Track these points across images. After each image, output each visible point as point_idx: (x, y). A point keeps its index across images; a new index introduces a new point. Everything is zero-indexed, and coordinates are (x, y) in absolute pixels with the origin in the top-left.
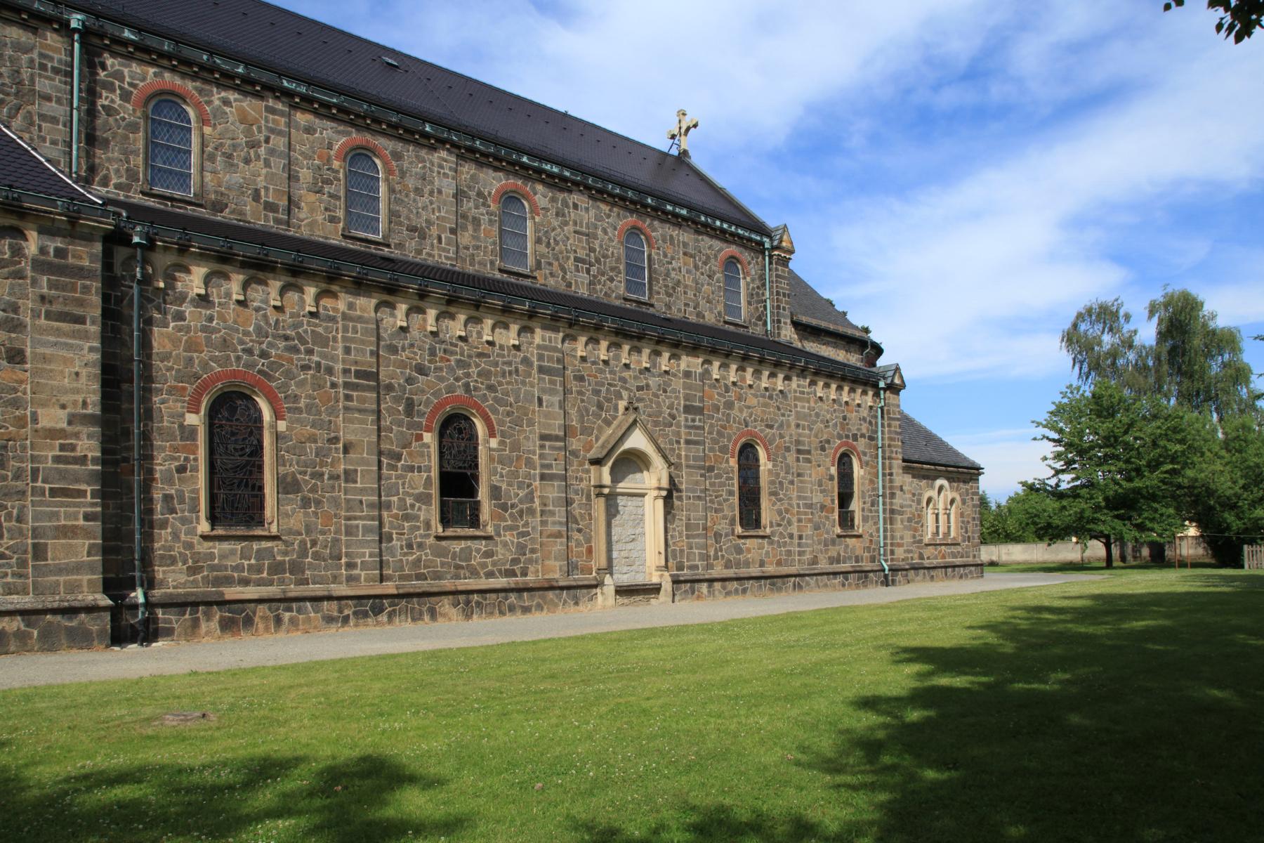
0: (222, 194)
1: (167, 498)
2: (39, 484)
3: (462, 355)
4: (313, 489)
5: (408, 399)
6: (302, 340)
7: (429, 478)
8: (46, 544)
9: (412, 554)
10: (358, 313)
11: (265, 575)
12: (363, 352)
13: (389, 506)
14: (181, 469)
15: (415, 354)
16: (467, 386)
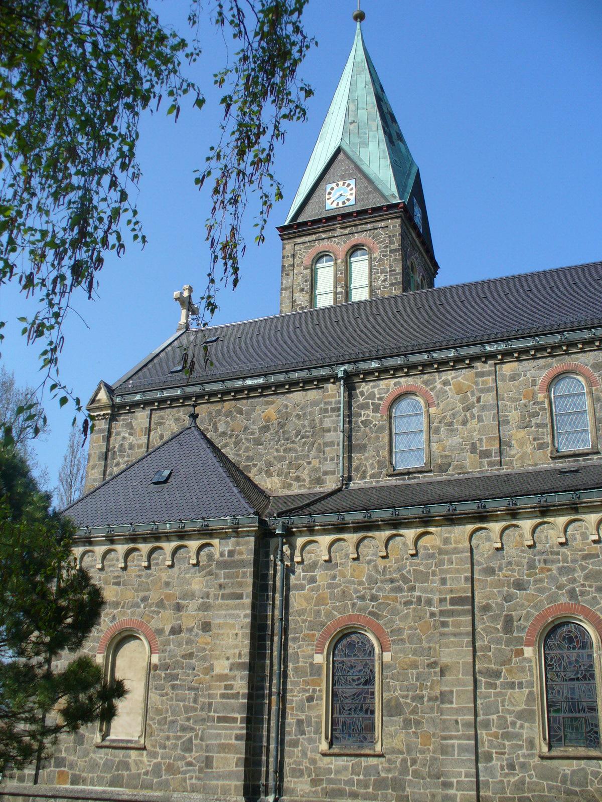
0: (446, 456)
1: (300, 722)
2: (212, 714)
3: (565, 561)
4: (414, 711)
5: (506, 616)
6: (405, 579)
7: (531, 693)
8: (213, 757)
9: (514, 775)
10: (454, 545)
11: (371, 790)
12: (458, 580)
13: (487, 725)
14: (310, 699)
15: (513, 571)
16: (572, 594)
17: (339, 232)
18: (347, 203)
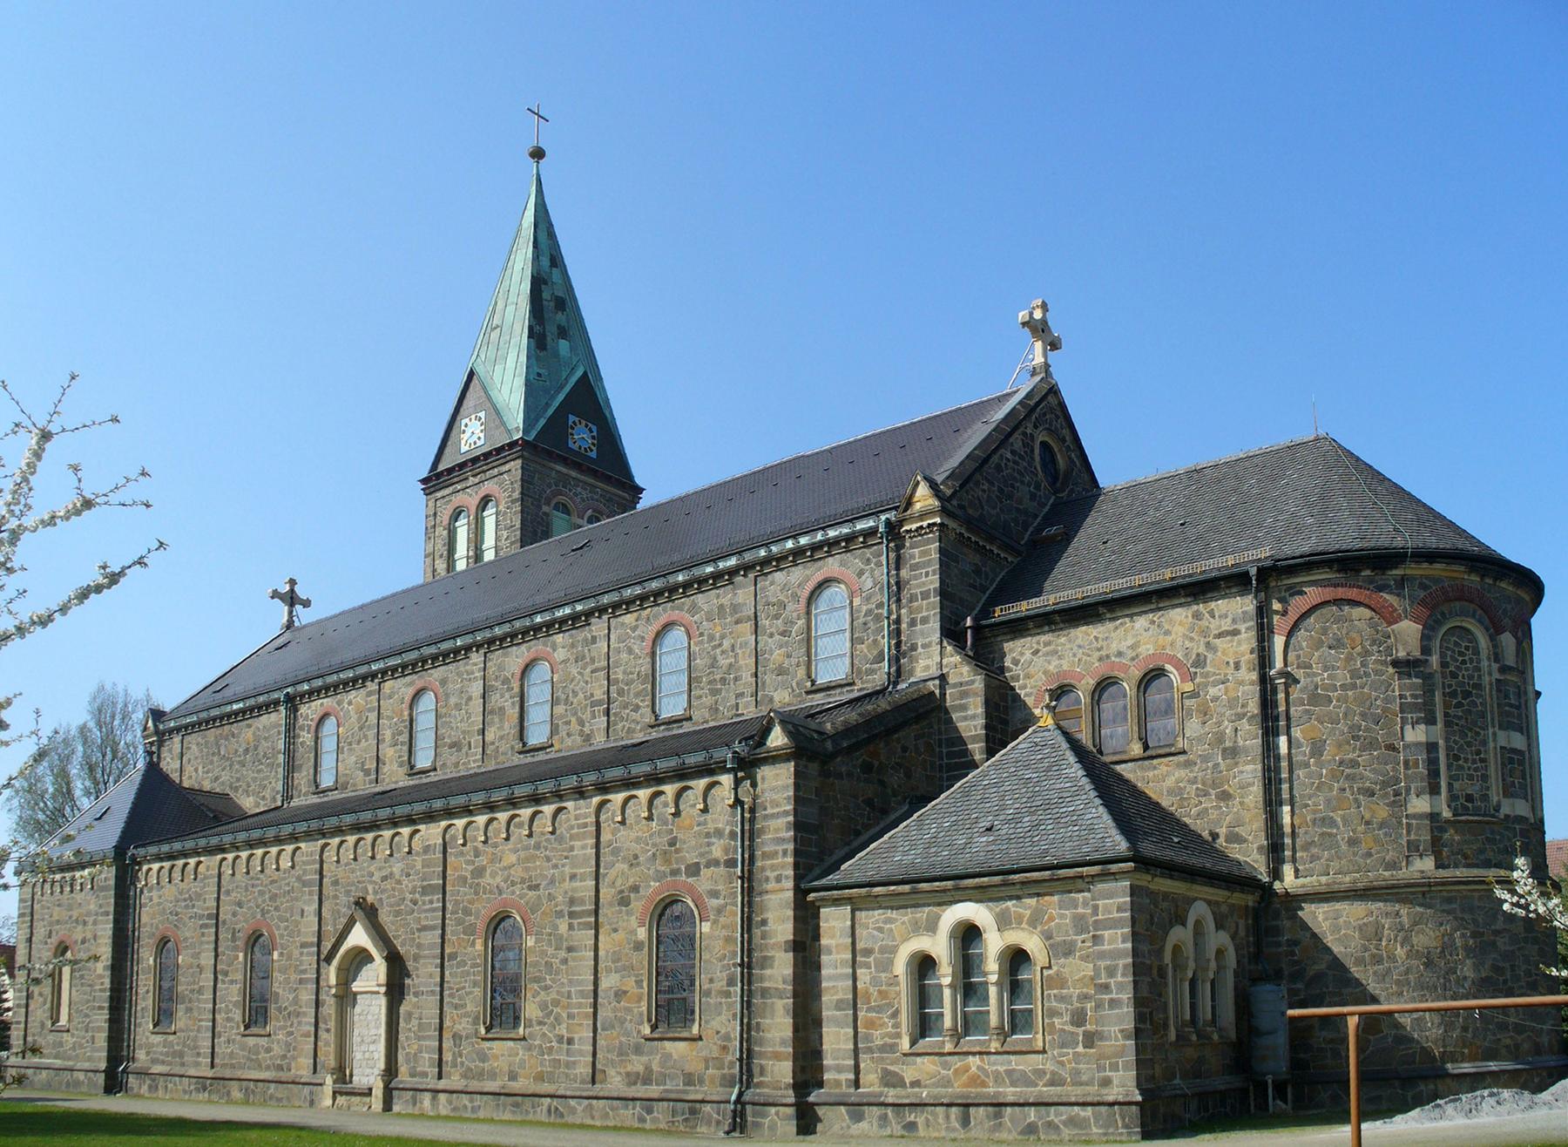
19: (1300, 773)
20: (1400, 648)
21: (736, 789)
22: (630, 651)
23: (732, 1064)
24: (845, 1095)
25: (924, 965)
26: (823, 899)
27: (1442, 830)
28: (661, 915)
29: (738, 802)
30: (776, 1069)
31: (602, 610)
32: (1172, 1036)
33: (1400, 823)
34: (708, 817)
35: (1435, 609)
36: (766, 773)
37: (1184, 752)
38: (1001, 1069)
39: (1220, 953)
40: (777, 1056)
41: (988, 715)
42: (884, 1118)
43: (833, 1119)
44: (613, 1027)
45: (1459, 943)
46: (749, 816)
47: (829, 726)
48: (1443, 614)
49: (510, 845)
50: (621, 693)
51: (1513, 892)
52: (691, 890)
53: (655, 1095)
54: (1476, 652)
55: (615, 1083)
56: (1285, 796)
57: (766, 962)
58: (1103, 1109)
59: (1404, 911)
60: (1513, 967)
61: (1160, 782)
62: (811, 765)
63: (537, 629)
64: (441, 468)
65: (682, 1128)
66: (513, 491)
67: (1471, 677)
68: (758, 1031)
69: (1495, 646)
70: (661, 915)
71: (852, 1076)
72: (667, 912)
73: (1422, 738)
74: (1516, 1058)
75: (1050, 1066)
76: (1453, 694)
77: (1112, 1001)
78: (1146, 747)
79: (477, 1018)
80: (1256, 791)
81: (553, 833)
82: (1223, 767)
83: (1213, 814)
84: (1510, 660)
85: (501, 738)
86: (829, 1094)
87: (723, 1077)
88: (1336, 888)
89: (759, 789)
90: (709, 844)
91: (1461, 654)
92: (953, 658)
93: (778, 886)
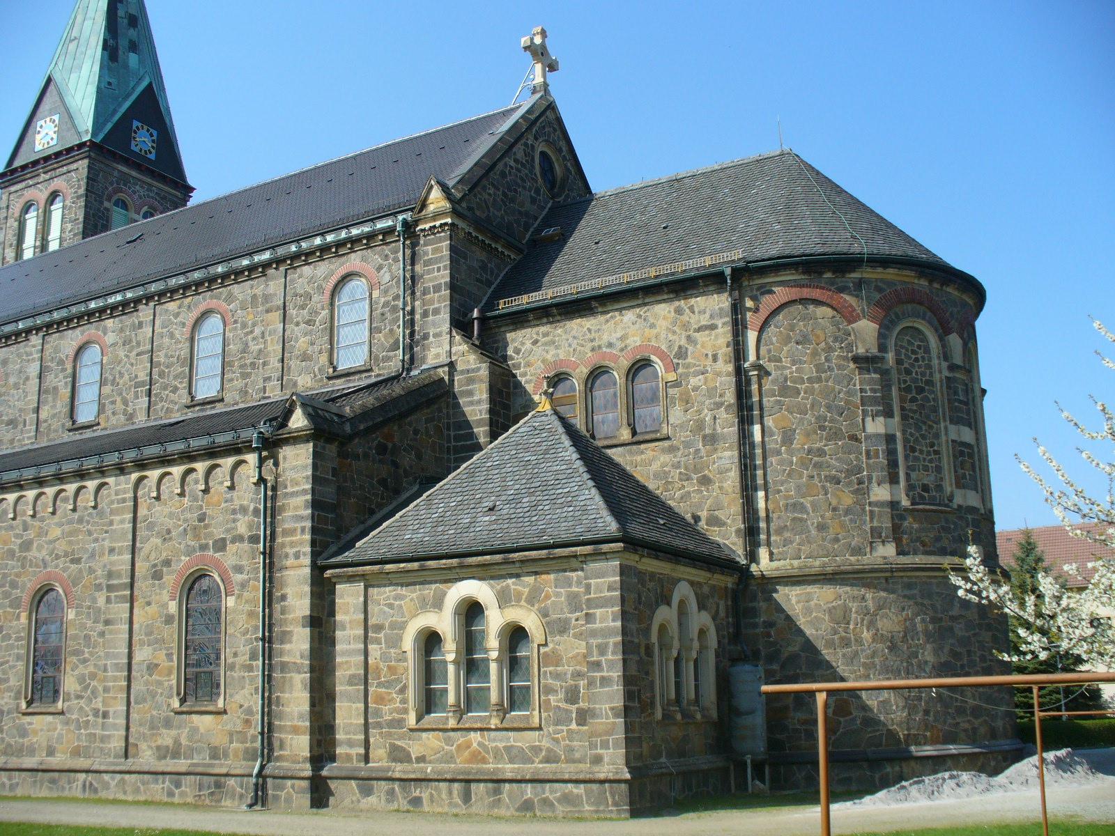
17: (41, 179)
18: (51, 144)
19: (773, 460)
20: (860, 346)
21: (260, 467)
22: (172, 336)
23: (254, 739)
24: (356, 769)
25: (431, 640)
26: (338, 576)
27: (902, 518)
28: (191, 588)
29: (261, 480)
30: (294, 742)
31: (149, 298)
32: (659, 715)
33: (864, 510)
34: (235, 494)
35: (890, 310)
36: (286, 452)
37: (668, 438)
38: (501, 745)
39: (702, 633)
40: (296, 730)
41: (492, 400)
42: (391, 793)
43: (345, 792)
44: (145, 700)
45: (920, 627)
46: (270, 490)
47: (347, 409)
48: (896, 314)
49: (56, 519)
50: (161, 374)
51: (967, 579)
52: (218, 565)
53: (183, 769)
54: (927, 350)
55: (146, 757)
56: (760, 481)
57: (285, 637)
58: (595, 786)
59: (869, 596)
60: (969, 652)
61: (646, 466)
62: (328, 446)
63: (90, 314)
64: (17, 164)
65: (207, 802)
66: (79, 187)
67: (923, 374)
68: (278, 706)
69: (944, 346)
70: (191, 588)
71: (362, 751)
72: (195, 585)
73: (882, 430)
74: (973, 741)
75: (546, 743)
76: (908, 390)
77: (603, 678)
78: (634, 433)
79: (19, 692)
80: (733, 477)
81: (95, 507)
82: (703, 453)
83: (695, 498)
84: (958, 360)
85: (54, 416)
86: (339, 768)
87: (246, 751)
88: (807, 571)
89: (280, 468)
90: (234, 521)
91: (913, 352)
92: (461, 347)
93: (296, 562)
